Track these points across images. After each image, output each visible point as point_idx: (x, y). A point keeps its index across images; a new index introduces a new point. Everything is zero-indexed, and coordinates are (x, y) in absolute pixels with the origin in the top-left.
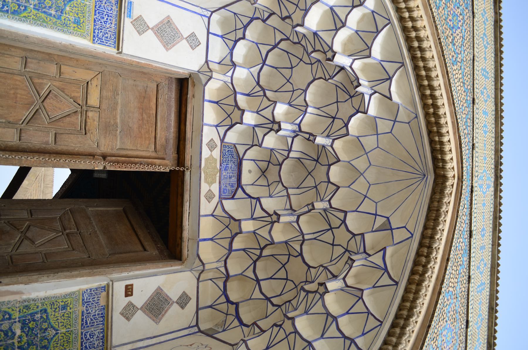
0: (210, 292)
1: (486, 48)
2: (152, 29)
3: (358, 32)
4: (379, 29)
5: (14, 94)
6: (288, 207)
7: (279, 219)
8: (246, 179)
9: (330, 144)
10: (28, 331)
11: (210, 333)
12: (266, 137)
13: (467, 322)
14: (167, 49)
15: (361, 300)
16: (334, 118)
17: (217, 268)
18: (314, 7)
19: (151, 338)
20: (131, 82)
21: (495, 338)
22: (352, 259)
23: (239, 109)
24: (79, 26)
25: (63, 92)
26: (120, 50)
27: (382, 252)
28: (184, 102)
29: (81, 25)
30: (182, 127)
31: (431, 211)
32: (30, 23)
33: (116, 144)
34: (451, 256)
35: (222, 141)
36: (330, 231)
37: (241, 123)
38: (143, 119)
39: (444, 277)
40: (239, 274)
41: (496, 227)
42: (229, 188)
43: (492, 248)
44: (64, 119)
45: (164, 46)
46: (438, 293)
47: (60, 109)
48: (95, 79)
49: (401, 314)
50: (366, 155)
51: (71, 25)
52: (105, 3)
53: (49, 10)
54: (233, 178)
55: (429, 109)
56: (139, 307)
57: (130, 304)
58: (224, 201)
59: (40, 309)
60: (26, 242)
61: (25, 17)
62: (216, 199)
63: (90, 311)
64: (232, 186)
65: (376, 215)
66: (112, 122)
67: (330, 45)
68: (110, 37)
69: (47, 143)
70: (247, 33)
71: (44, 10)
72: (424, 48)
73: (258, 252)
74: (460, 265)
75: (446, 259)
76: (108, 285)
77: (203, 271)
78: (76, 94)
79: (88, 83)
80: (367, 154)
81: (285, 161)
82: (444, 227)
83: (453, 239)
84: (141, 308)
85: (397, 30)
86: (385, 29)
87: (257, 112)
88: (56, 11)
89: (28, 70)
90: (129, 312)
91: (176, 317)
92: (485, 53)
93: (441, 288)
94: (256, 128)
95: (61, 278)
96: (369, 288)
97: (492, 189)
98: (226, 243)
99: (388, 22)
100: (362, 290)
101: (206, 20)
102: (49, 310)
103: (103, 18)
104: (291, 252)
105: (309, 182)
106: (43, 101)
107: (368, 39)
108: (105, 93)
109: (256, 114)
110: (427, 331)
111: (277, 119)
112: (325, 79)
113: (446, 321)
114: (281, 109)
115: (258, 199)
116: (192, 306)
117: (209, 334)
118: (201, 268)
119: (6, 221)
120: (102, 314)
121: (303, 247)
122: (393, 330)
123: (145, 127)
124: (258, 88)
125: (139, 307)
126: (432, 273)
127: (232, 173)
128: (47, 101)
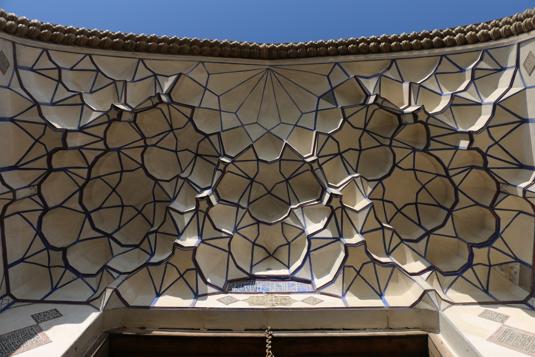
36: (343, 155)
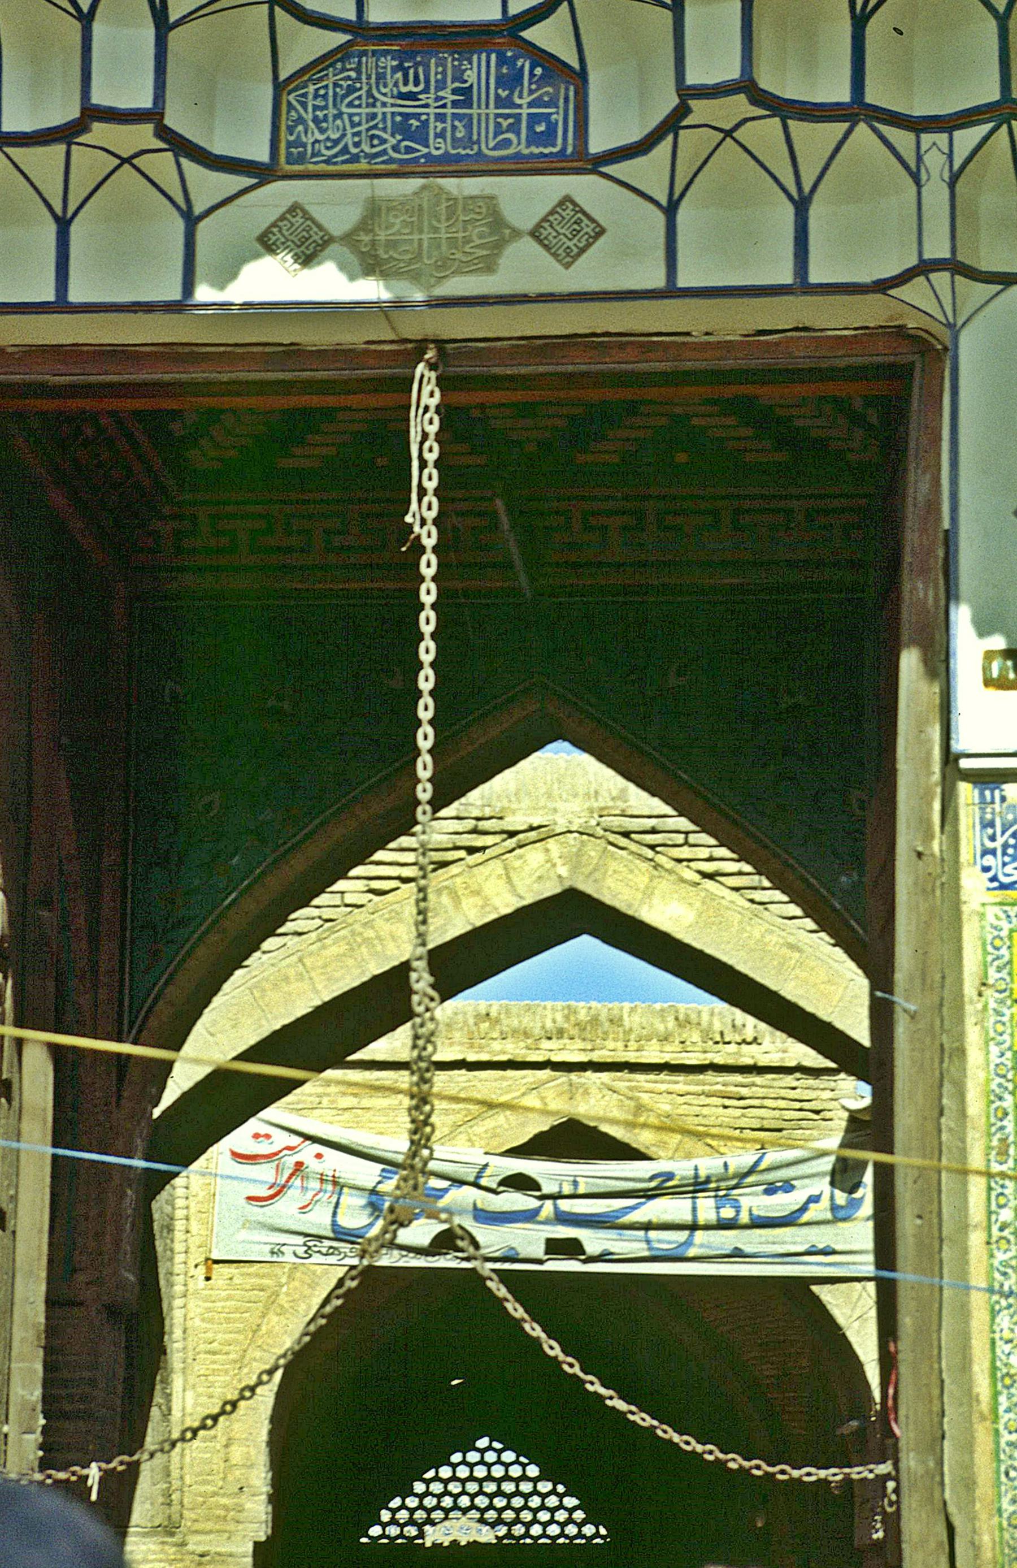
35: (263, 173)
37: (154, 116)
58: (597, 145)
62: (583, 187)
64: (511, 81)
98: (815, 139)
127: (441, 85)
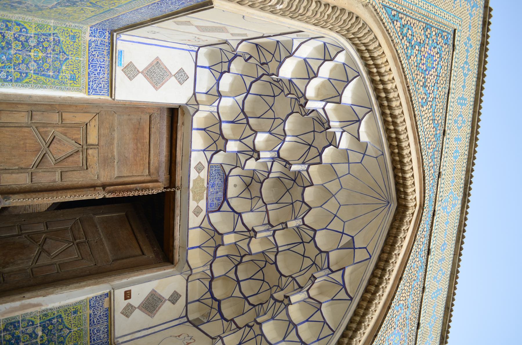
0: (197, 289)
1: (465, 75)
2: (142, 72)
3: (331, 80)
4: (349, 80)
5: (23, 144)
6: (266, 221)
7: (256, 235)
8: (231, 192)
9: (306, 169)
10: (48, 332)
11: (197, 323)
12: (247, 161)
13: (419, 324)
14: (157, 89)
15: (319, 311)
16: (311, 146)
17: (203, 271)
18: (287, 60)
19: (147, 329)
20: (125, 117)
21: (448, 332)
22: (314, 277)
23: (223, 138)
24: (75, 82)
25: (66, 136)
26: (113, 98)
27: (342, 271)
28: (174, 129)
29: (77, 80)
30: (174, 151)
31: (390, 236)
32: (32, 88)
33: (114, 174)
34: (404, 276)
35: (209, 162)
38: (137, 149)
39: (395, 293)
40: (223, 275)
41: (459, 239)
42: (215, 202)
43: (454, 258)
44: (67, 159)
45: (154, 87)
46: (387, 307)
47: (63, 151)
48: (93, 120)
49: (351, 327)
50: (338, 180)
51: (68, 81)
52: (98, 56)
53: (47, 72)
54: (220, 193)
55: (395, 149)
56: (137, 307)
57: (129, 305)
58: (211, 215)
59: (56, 315)
60: (43, 254)
61: (27, 82)
62: (204, 213)
63: (96, 313)
64: (219, 200)
65: (343, 233)
66: (110, 155)
67: (303, 92)
68: (104, 86)
69: (55, 181)
70: (233, 66)
71: (43, 73)
72: (391, 99)
73: (239, 259)
74: (414, 280)
75: (399, 278)
76: (110, 292)
77: (190, 275)
78: (77, 136)
79: (87, 125)
80: (339, 178)
81: (266, 180)
82: (400, 252)
83: (408, 260)
84: (138, 307)
85: (365, 82)
86: (355, 80)
87: (240, 140)
88: (54, 72)
89: (33, 121)
90: (128, 311)
91: (168, 311)
92: (464, 82)
93: (391, 304)
94: (239, 154)
95: (72, 289)
96: (328, 301)
97: (460, 206)
98: (211, 251)
99: (358, 74)
100: (321, 303)
101: (194, 54)
102: (63, 316)
103: (96, 70)
104: (266, 261)
105: (287, 199)
106: (48, 147)
107: (339, 86)
108: (102, 131)
109: (238, 142)
110: (374, 340)
111: (257, 148)
112: (302, 115)
113: (395, 328)
114: (261, 138)
115: (240, 214)
116: (182, 301)
117: (196, 324)
118: (189, 272)
119: (27, 235)
120: (106, 314)
121: (277, 257)
122: (342, 340)
123: (139, 155)
124: (242, 116)
125: (137, 307)
126: (383, 292)
128: (52, 146)
